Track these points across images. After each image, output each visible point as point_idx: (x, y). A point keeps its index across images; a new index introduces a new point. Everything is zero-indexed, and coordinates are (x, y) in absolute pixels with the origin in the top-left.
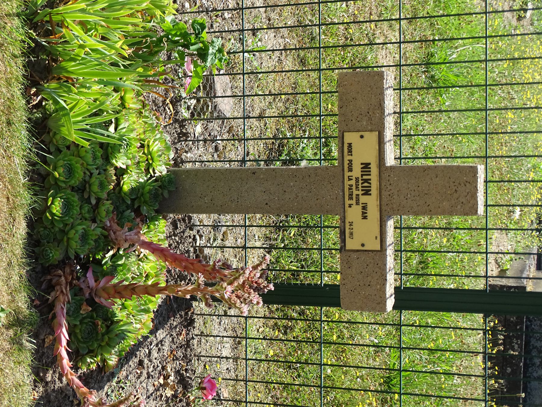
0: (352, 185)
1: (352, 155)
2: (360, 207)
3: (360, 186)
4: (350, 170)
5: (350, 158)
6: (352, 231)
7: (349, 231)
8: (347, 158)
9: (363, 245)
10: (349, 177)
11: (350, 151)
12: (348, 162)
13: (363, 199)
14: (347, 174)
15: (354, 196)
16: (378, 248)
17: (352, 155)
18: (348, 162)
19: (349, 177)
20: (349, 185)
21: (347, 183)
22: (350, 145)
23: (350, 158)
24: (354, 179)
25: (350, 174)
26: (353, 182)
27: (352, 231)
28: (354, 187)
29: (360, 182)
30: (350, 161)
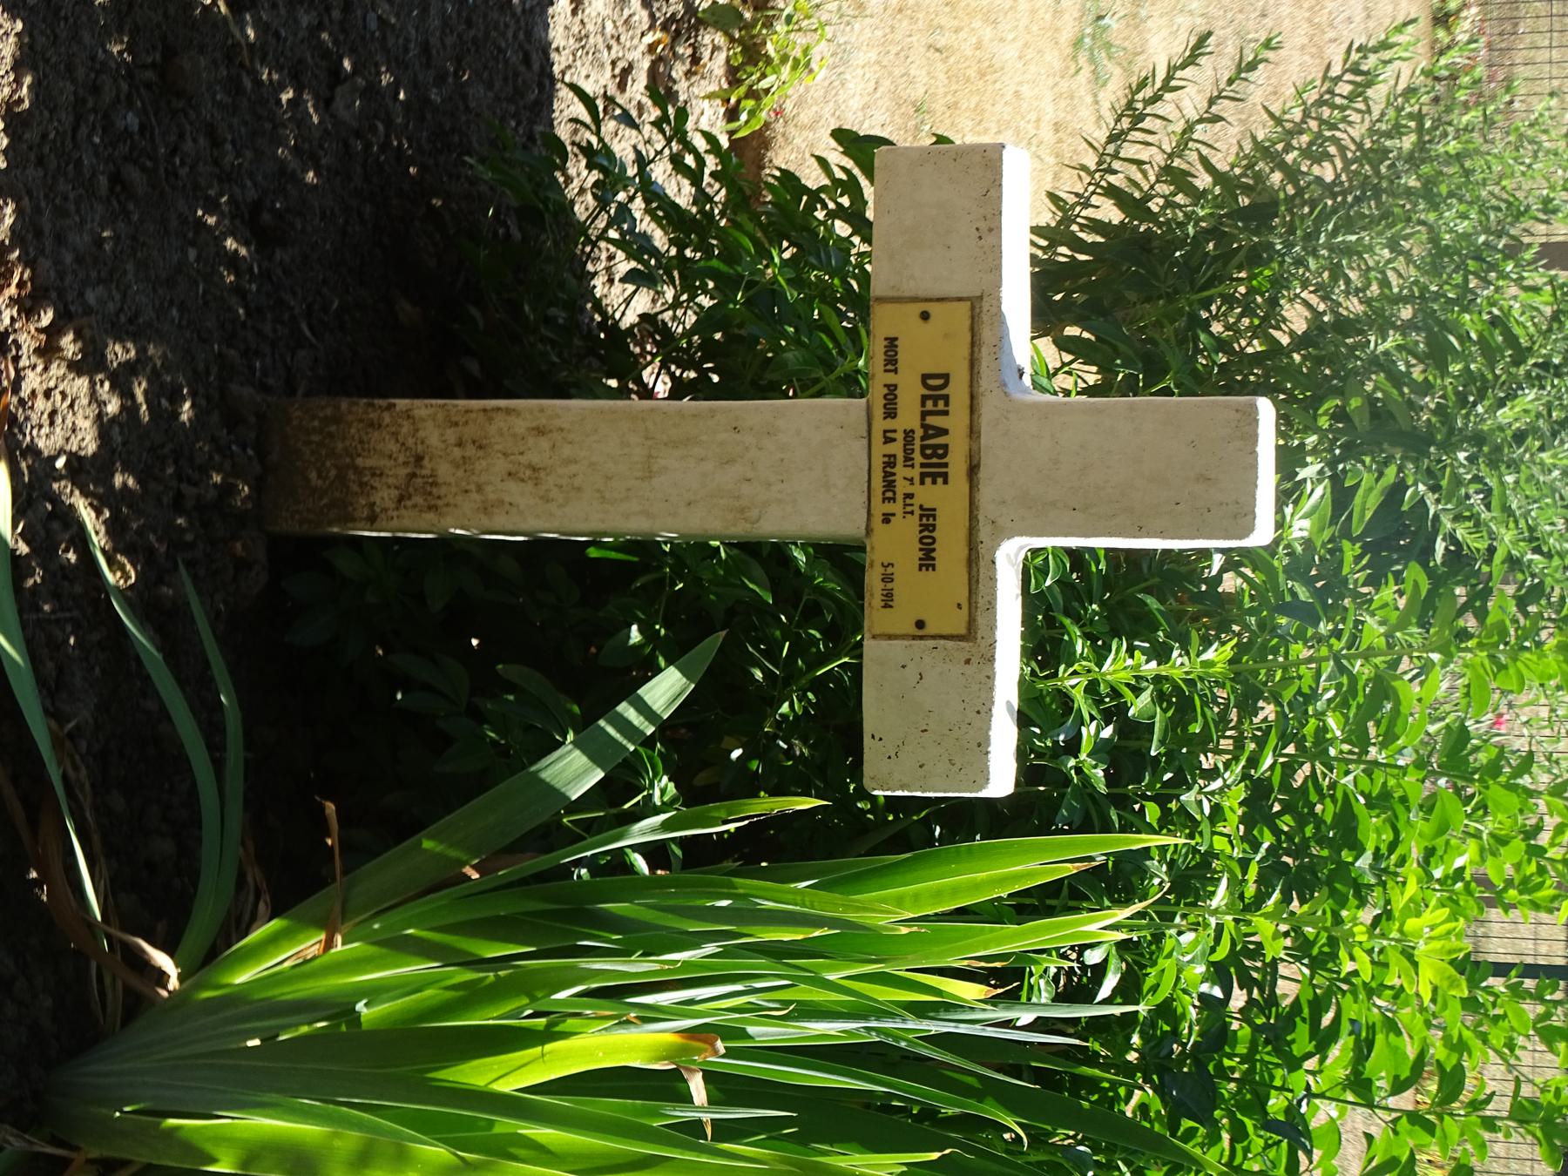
1: (895, 371)
2: (913, 523)
3: (918, 458)
4: (891, 413)
5: (891, 378)
6: (889, 586)
7: (882, 585)
8: (881, 379)
9: (920, 624)
10: (885, 432)
11: (891, 362)
12: (885, 391)
13: (928, 494)
14: (880, 424)
16: (963, 631)
17: (895, 371)
18: (885, 391)
19: (885, 432)
20: (889, 456)
22: (892, 343)
23: (891, 378)
24: (900, 436)
25: (890, 424)
26: (897, 448)
27: (889, 586)
29: (917, 444)
30: (892, 389)
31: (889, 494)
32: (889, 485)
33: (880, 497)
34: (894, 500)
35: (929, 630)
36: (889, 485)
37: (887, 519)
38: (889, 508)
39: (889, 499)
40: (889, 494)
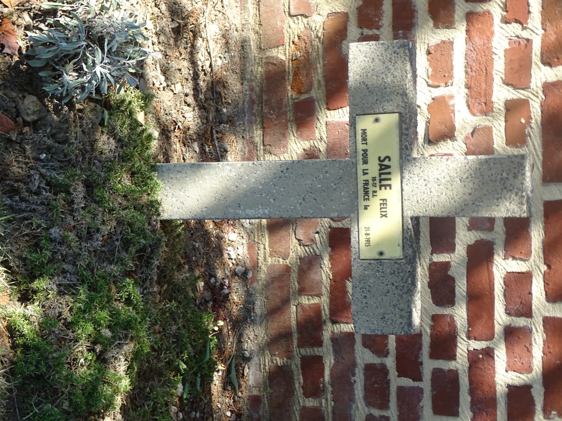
0: (368, 180)
1: (366, 144)
4: (365, 162)
6: (368, 237)
7: (365, 237)
10: (364, 170)
11: (364, 139)
12: (363, 152)
14: (361, 167)
15: (371, 194)
17: (366, 144)
18: (363, 152)
20: (366, 181)
21: (361, 178)
22: (364, 131)
25: (365, 167)
27: (368, 237)
28: (371, 182)
30: (365, 151)
31: (366, 197)
32: (366, 193)
33: (363, 198)
34: (369, 199)
35: (386, 256)
36: (366, 193)
37: (366, 208)
38: (366, 203)
39: (367, 199)
40: (366, 197)
